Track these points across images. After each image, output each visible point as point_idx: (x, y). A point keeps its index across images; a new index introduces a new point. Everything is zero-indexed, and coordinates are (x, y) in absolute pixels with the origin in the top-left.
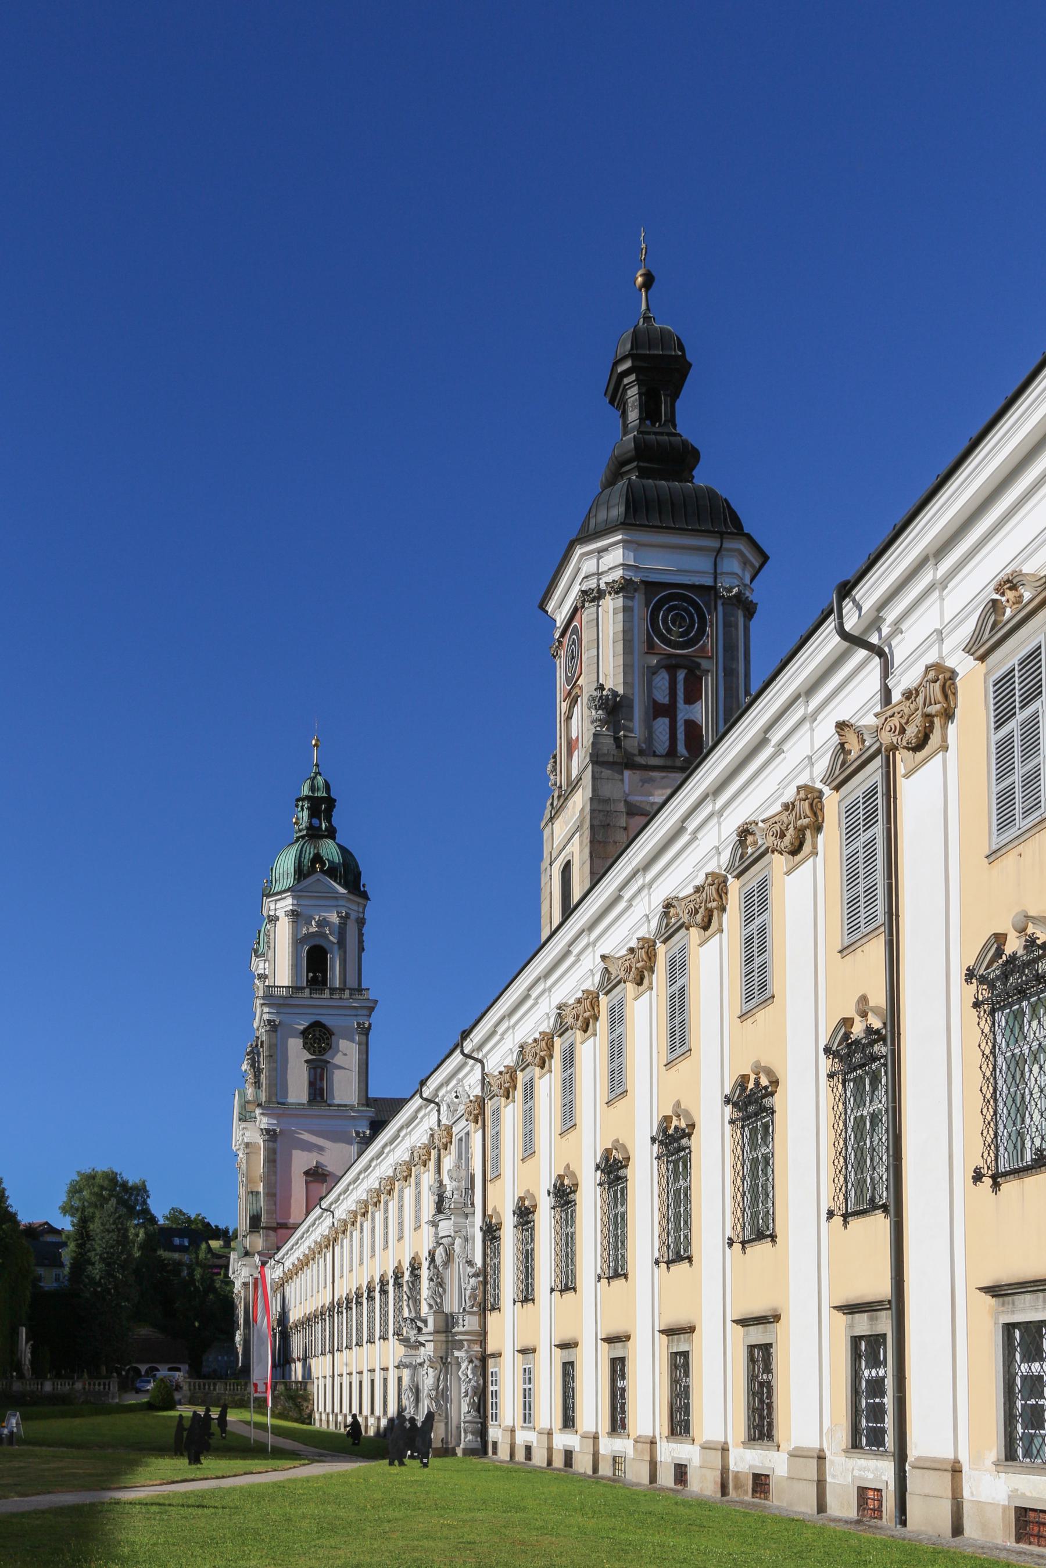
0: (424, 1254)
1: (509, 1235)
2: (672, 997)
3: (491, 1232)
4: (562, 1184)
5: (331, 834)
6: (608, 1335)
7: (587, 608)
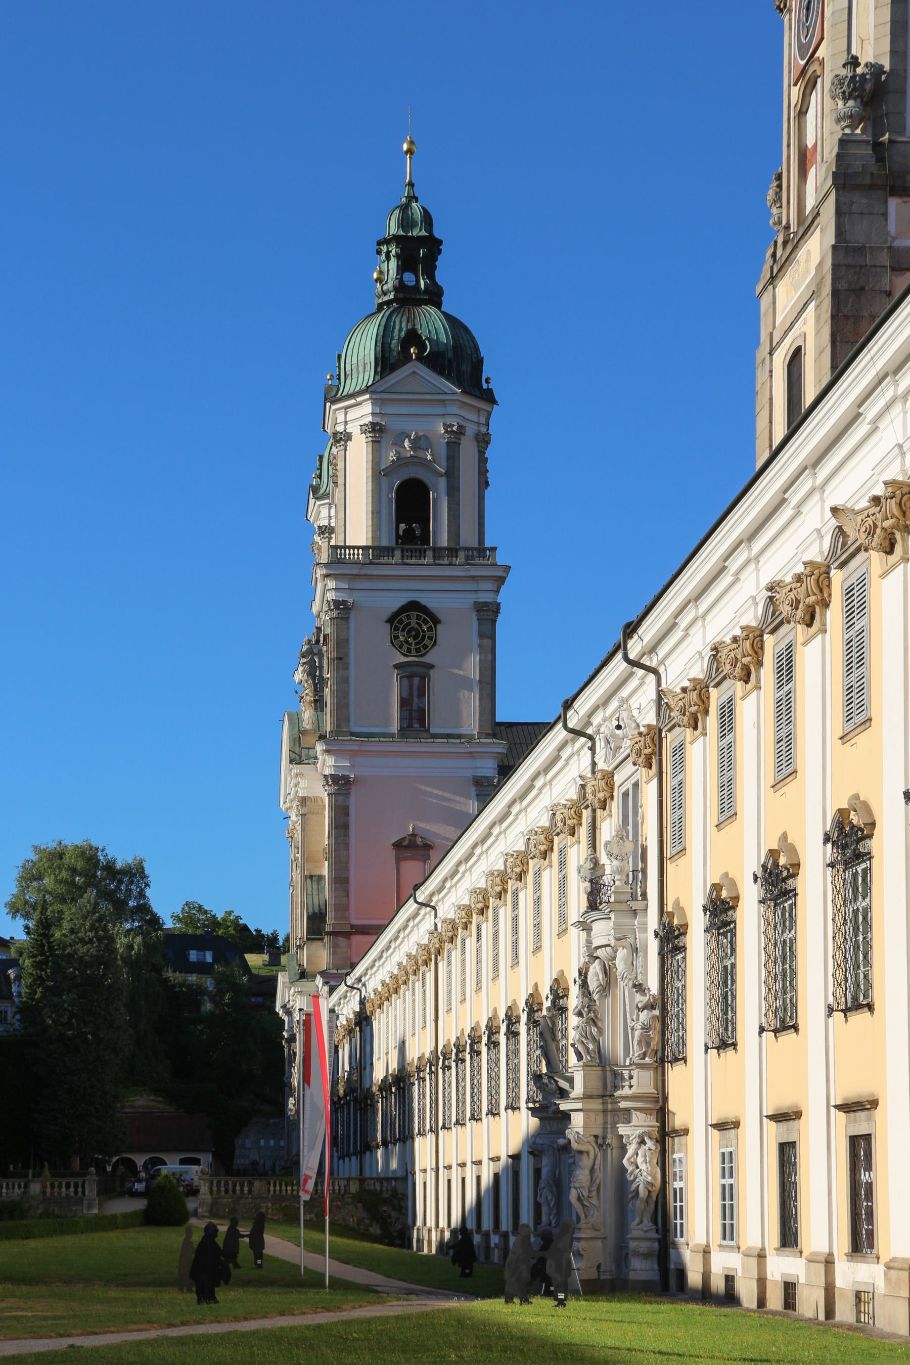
0: (572, 974)
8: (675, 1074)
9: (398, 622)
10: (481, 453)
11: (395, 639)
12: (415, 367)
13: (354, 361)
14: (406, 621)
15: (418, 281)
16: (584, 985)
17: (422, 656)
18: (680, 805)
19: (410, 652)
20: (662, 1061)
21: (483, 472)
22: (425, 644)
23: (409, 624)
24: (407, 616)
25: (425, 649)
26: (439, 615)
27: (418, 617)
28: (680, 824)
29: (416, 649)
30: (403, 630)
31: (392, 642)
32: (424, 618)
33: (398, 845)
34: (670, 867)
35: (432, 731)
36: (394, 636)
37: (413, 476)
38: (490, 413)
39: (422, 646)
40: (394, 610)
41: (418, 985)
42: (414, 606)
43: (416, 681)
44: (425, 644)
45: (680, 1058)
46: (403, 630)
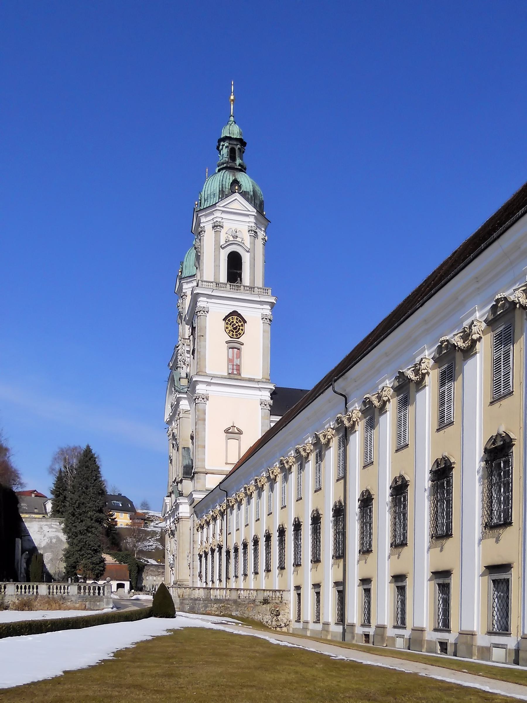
9: (228, 320)
11: (227, 329)
12: (237, 196)
14: (231, 320)
19: (233, 336)
22: (239, 333)
23: (233, 322)
24: (232, 318)
25: (240, 335)
29: (236, 335)
30: (230, 324)
31: (225, 331)
32: (239, 320)
33: (227, 431)
35: (243, 375)
36: (226, 327)
37: (235, 250)
39: (239, 334)
42: (234, 313)
44: (239, 333)
46: (230, 324)
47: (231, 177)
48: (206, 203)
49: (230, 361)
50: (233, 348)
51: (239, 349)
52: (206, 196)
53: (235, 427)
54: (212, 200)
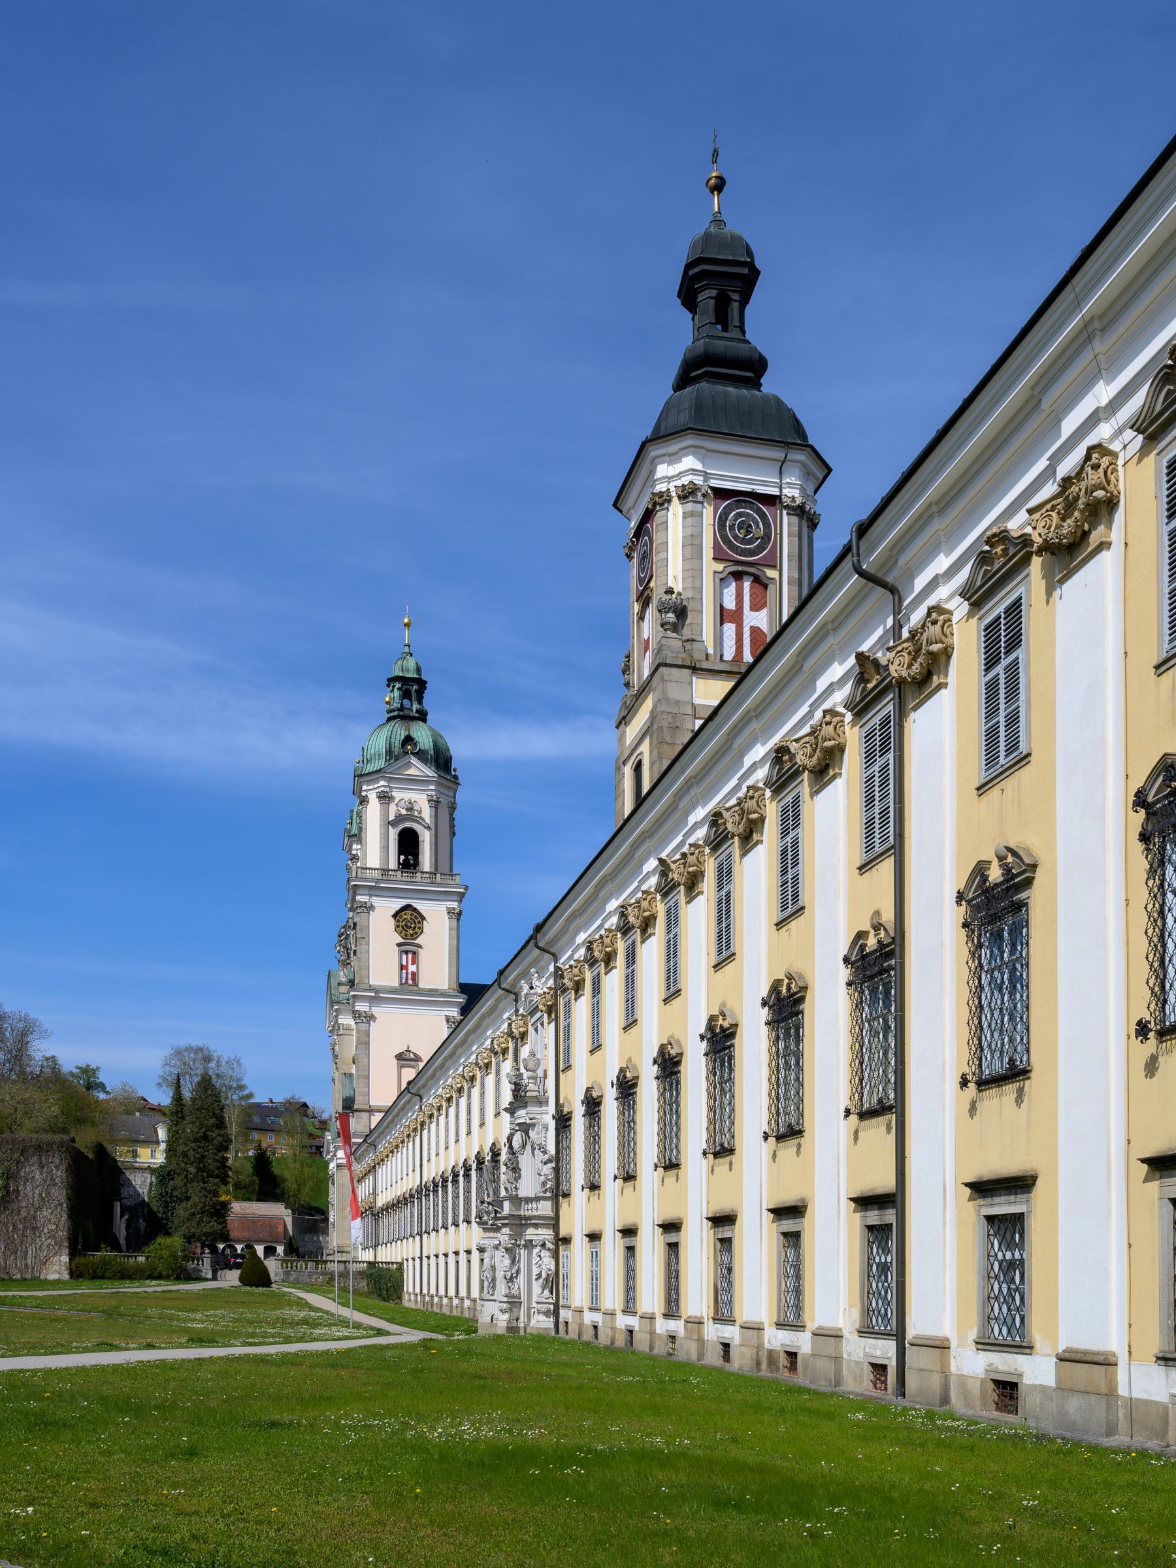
0: (504, 1140)
1: (579, 1124)
2: (720, 902)
3: (563, 1121)
4: (625, 1077)
5: (422, 716)
6: (664, 1221)
7: (659, 511)
8: (564, 1203)
10: (451, 814)
13: (373, 752)
15: (412, 705)
16: (511, 1147)
17: (414, 939)
18: (568, 1037)
20: (557, 1196)
21: (452, 826)
26: (424, 914)
27: (412, 915)
28: (568, 1049)
33: (400, 1057)
34: (562, 1076)
38: (456, 790)
40: (397, 909)
41: (411, 1144)
42: (408, 907)
43: (410, 956)
45: (566, 1195)
47: (403, 732)
48: (369, 764)
49: (402, 967)
50: (407, 952)
51: (414, 953)
52: (369, 756)
53: (410, 1051)
54: (377, 761)
